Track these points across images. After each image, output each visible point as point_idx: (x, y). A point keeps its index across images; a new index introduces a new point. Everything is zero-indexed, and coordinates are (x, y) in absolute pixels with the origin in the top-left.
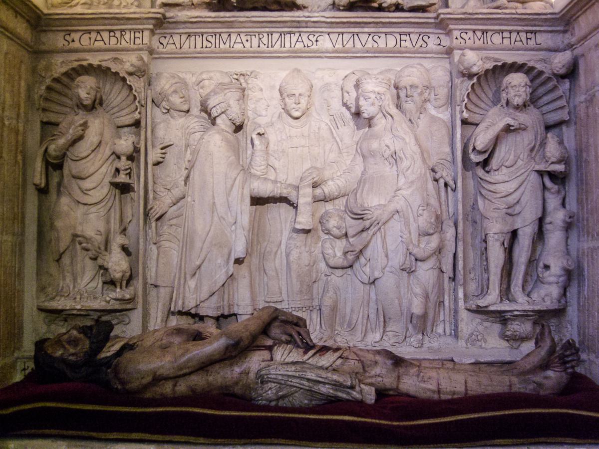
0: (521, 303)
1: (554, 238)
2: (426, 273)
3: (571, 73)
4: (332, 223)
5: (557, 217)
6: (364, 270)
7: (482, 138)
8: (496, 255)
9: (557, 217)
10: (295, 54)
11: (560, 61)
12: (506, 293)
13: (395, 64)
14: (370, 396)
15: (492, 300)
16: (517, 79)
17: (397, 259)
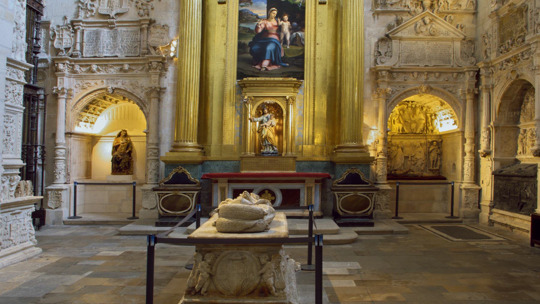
0: (435, 168)
1: (439, 161)
2: (424, 165)
3: (442, 142)
4: (413, 159)
5: (439, 158)
6: (417, 165)
7: (431, 149)
8: (432, 163)
9: (439, 158)
10: (408, 139)
11: (440, 140)
12: (433, 167)
13: (420, 140)
14: (420, 176)
15: (431, 168)
16: (435, 142)
17: (420, 164)
